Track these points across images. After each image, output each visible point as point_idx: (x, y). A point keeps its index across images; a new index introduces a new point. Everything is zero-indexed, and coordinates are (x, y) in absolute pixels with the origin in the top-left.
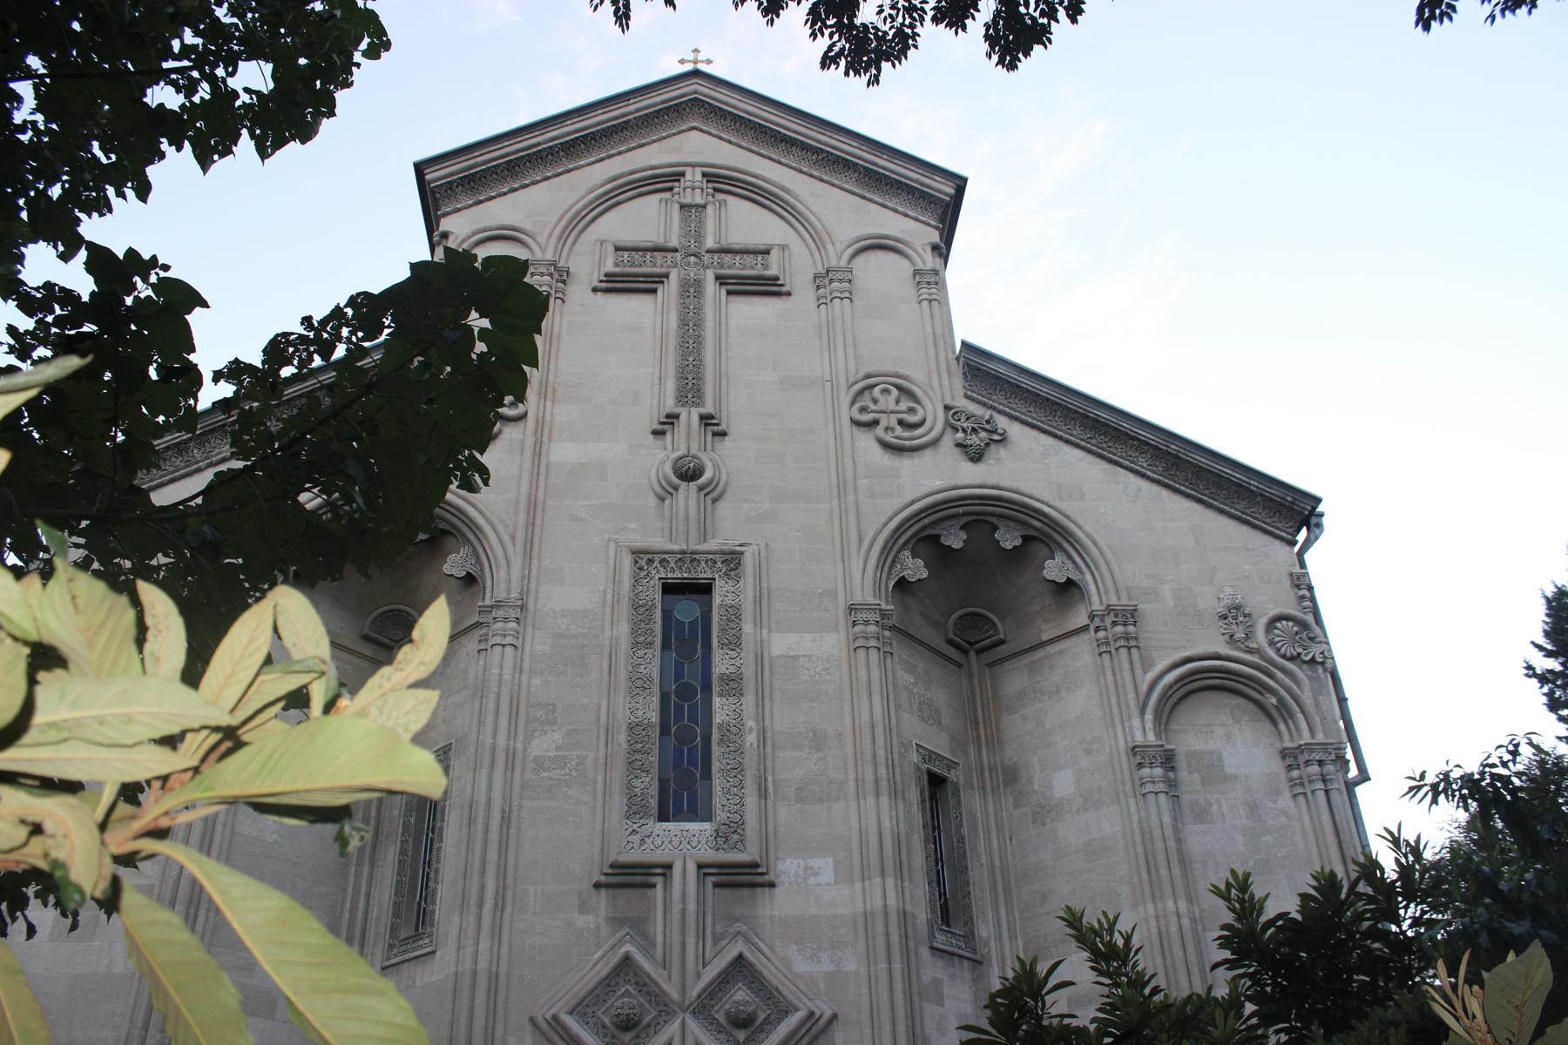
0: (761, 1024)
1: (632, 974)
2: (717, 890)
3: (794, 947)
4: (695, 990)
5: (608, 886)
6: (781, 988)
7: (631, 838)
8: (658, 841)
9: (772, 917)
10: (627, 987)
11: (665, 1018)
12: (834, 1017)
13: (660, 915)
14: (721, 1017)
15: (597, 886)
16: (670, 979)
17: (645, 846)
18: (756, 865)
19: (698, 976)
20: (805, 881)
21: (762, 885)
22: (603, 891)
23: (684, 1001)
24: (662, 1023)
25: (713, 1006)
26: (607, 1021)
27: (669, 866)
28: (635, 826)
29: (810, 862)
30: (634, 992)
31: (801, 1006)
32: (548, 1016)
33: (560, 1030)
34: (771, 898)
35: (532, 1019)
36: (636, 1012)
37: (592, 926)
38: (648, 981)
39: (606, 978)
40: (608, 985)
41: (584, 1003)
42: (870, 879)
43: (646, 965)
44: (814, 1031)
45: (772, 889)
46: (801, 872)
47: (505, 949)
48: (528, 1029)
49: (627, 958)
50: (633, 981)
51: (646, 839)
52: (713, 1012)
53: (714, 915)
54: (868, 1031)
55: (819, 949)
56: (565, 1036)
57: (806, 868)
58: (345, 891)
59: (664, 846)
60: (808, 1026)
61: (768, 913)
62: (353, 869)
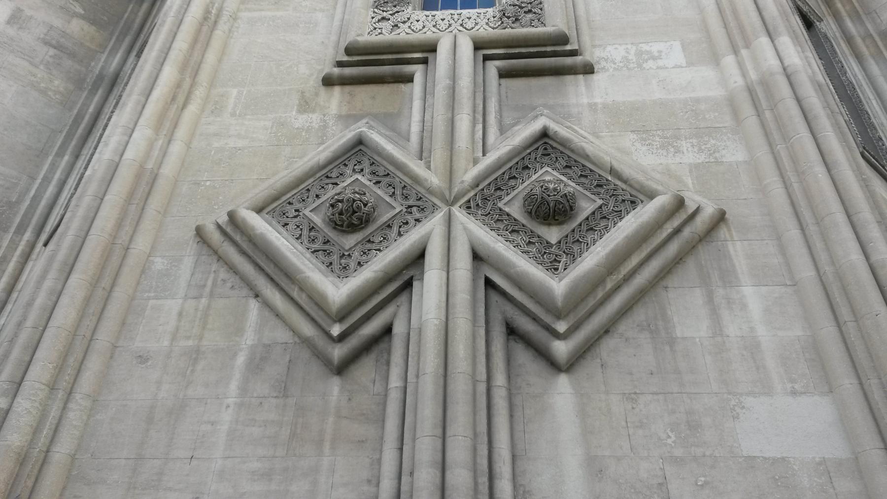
0: (587, 219)
1: (366, 164)
2: (503, 81)
3: (633, 136)
4: (468, 175)
5: (344, 82)
6: (616, 165)
7: (378, 25)
8: (419, 26)
9: (592, 107)
10: (359, 177)
11: (418, 215)
12: (721, 218)
13: (417, 104)
14: (516, 210)
15: (328, 82)
16: (429, 168)
17: (398, 31)
18: (563, 39)
19: (475, 162)
20: (640, 66)
21: (572, 71)
22: (337, 89)
23: (450, 188)
24: (412, 222)
25: (500, 198)
26: (317, 219)
27: (431, 48)
28: (385, 14)
29: (645, 47)
30: (368, 183)
31: (660, 188)
32: (223, 219)
33: (238, 238)
34: (588, 86)
35: (199, 232)
36: (365, 198)
37: (315, 125)
38: (391, 168)
39: (324, 167)
40: (327, 177)
41: (284, 198)
42: (747, 46)
43: (389, 148)
44: (687, 232)
45: (589, 76)
46: (632, 57)
47: (176, 148)
48: (192, 248)
49: (359, 144)
50: (367, 171)
51: (401, 25)
52: (500, 205)
53: (500, 102)
54: (793, 233)
55: (677, 138)
56: (245, 245)
57: (639, 53)
58: (33, 178)
59: (425, 30)
60: (676, 222)
61: (585, 100)
62: (50, 158)
